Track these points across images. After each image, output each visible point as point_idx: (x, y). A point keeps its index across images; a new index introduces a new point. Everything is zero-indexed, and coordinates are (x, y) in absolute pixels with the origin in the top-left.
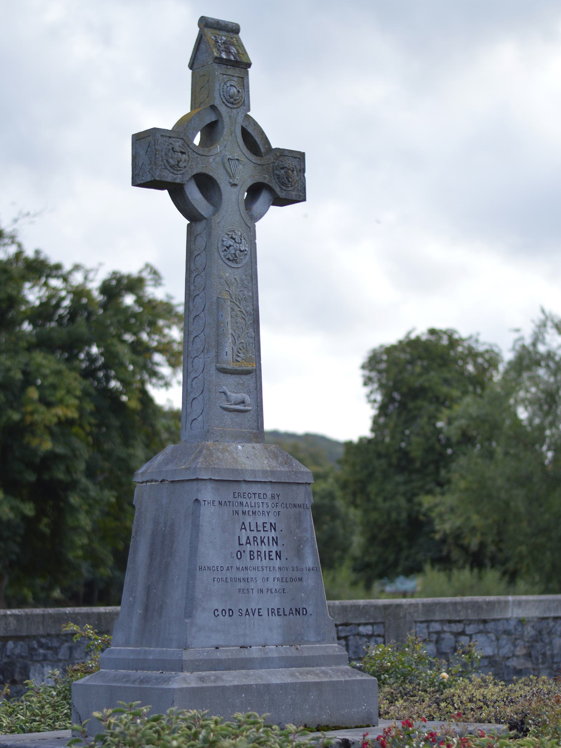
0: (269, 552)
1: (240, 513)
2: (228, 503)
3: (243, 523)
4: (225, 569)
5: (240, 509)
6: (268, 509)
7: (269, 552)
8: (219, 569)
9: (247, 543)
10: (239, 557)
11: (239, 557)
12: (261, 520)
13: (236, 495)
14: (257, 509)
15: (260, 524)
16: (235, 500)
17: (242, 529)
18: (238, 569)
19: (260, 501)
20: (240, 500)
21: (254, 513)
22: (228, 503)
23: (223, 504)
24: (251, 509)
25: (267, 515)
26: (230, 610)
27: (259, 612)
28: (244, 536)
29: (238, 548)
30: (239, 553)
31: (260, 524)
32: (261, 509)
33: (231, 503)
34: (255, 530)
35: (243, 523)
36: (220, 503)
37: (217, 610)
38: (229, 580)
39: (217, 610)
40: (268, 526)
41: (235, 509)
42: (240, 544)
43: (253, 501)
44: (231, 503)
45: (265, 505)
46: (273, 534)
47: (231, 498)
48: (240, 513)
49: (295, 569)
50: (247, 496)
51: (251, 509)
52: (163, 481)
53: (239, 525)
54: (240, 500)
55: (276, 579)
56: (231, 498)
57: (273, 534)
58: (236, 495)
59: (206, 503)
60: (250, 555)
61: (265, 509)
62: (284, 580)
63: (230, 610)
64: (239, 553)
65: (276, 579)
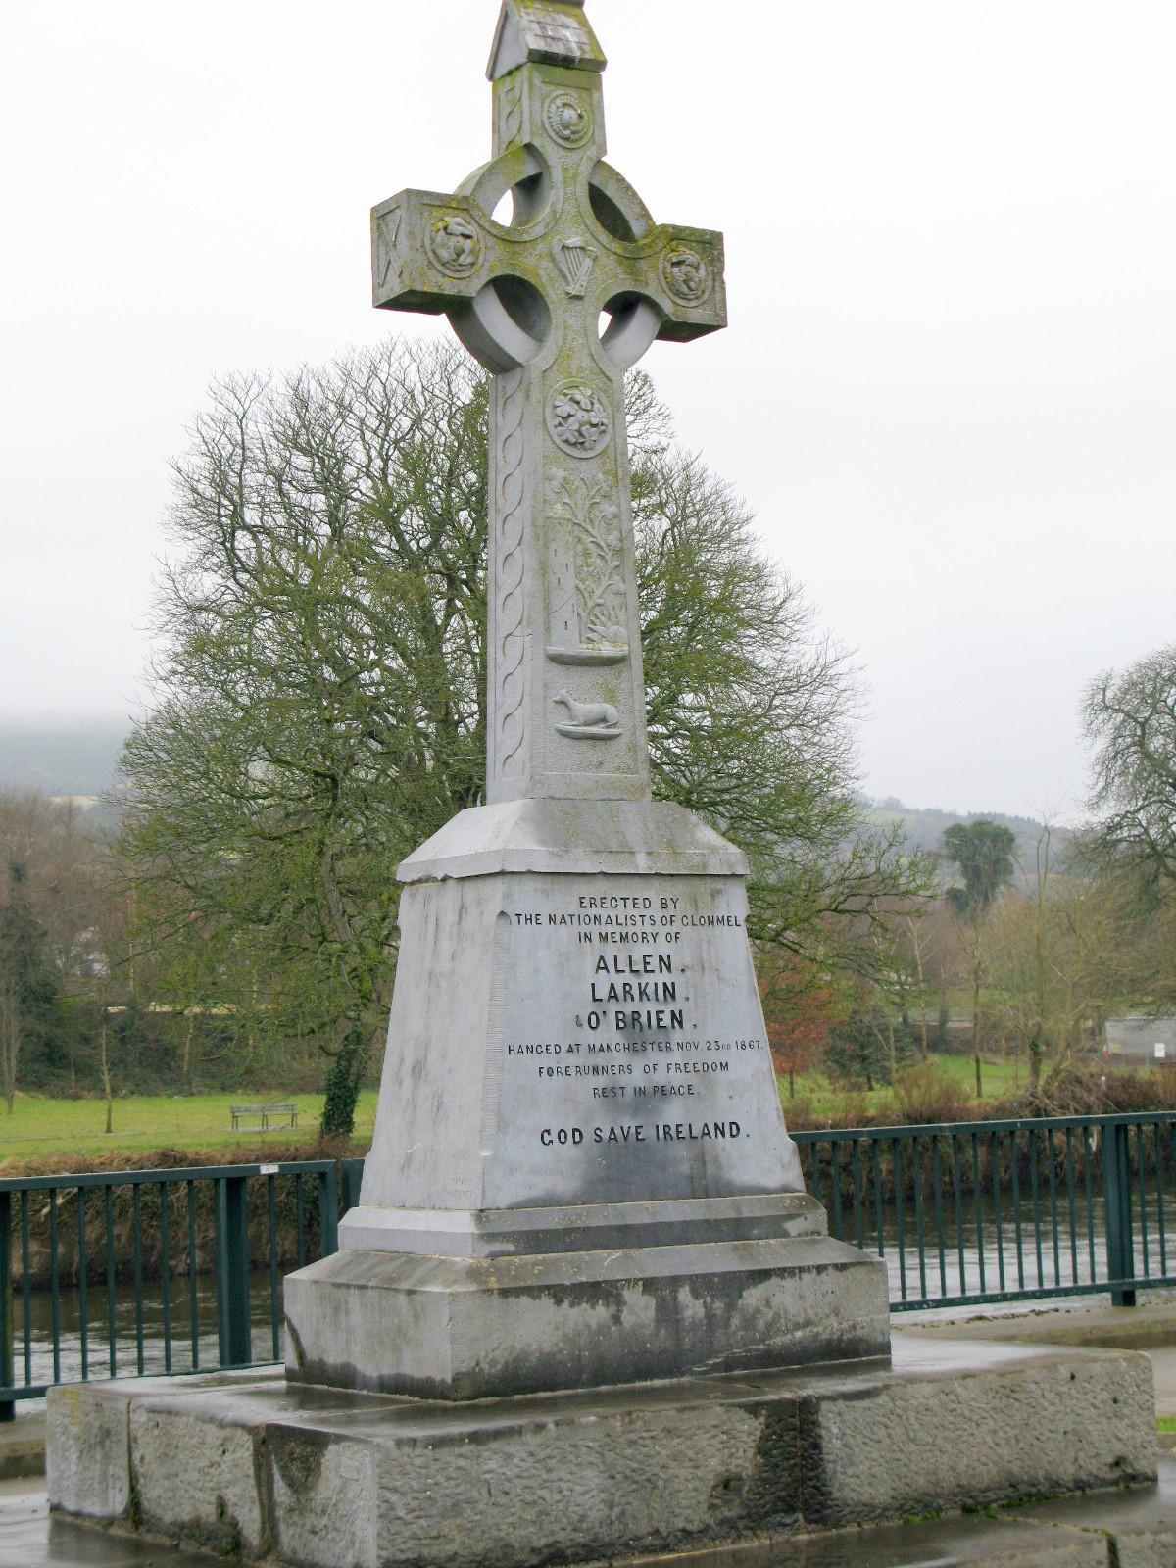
0: (658, 1013)
1: (595, 938)
2: (568, 919)
3: (602, 957)
4: (565, 1048)
5: (595, 930)
6: (654, 930)
7: (658, 1013)
8: (552, 1049)
9: (610, 997)
10: (594, 1025)
11: (594, 1025)
12: (638, 951)
13: (586, 903)
14: (631, 930)
15: (637, 958)
16: (583, 912)
17: (599, 968)
18: (592, 1048)
19: (637, 913)
20: (593, 912)
21: (624, 938)
22: (568, 919)
23: (558, 921)
24: (617, 929)
25: (650, 938)
26: (575, 1130)
27: (638, 1133)
28: (603, 982)
29: (591, 1007)
30: (593, 1018)
31: (637, 958)
32: (638, 929)
33: (575, 919)
34: (627, 969)
35: (602, 957)
36: (552, 919)
37: (548, 1131)
38: (572, 1071)
39: (548, 1131)
40: (654, 963)
41: (584, 929)
42: (595, 1000)
43: (621, 912)
44: (575, 919)
45: (647, 919)
46: (665, 977)
47: (575, 909)
48: (595, 938)
49: (713, 1045)
50: (607, 904)
51: (617, 929)
52: (445, 879)
53: (591, 962)
54: (593, 912)
55: (673, 1067)
56: (575, 909)
57: (665, 977)
58: (586, 903)
59: (523, 919)
60: (618, 1020)
61: (648, 928)
62: (690, 1068)
63: (575, 1130)
64: (593, 1018)
65: (673, 1067)
